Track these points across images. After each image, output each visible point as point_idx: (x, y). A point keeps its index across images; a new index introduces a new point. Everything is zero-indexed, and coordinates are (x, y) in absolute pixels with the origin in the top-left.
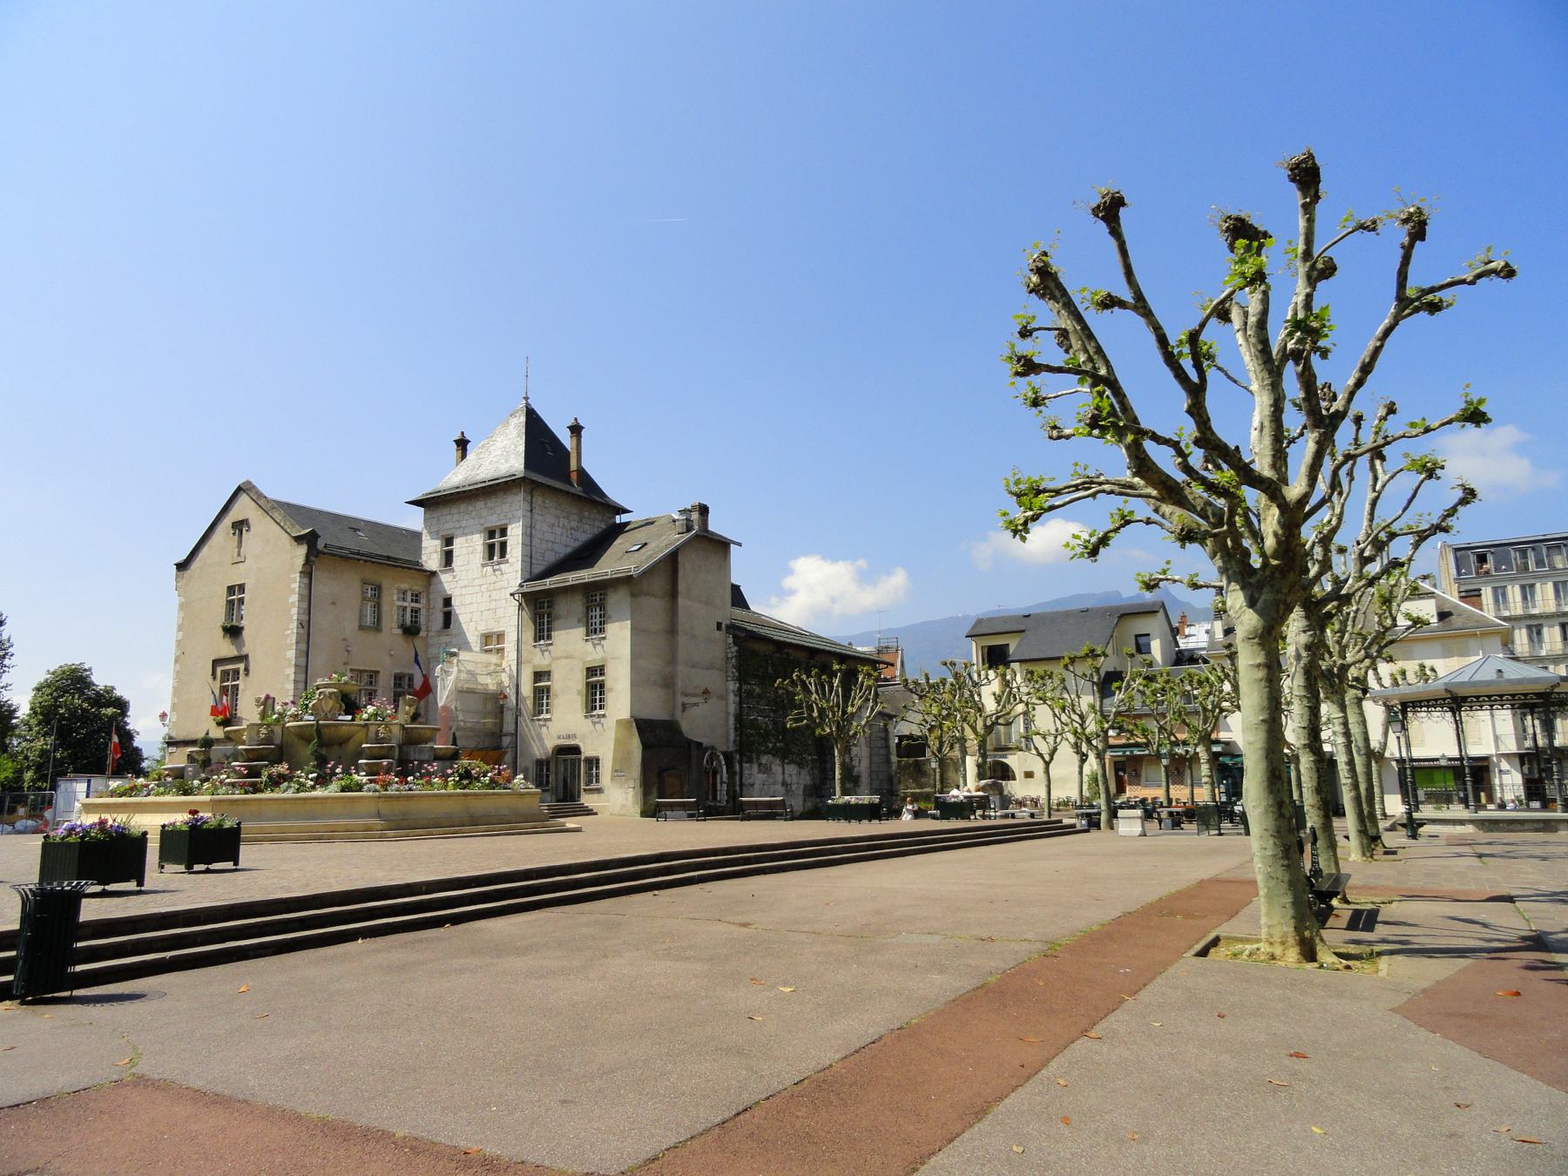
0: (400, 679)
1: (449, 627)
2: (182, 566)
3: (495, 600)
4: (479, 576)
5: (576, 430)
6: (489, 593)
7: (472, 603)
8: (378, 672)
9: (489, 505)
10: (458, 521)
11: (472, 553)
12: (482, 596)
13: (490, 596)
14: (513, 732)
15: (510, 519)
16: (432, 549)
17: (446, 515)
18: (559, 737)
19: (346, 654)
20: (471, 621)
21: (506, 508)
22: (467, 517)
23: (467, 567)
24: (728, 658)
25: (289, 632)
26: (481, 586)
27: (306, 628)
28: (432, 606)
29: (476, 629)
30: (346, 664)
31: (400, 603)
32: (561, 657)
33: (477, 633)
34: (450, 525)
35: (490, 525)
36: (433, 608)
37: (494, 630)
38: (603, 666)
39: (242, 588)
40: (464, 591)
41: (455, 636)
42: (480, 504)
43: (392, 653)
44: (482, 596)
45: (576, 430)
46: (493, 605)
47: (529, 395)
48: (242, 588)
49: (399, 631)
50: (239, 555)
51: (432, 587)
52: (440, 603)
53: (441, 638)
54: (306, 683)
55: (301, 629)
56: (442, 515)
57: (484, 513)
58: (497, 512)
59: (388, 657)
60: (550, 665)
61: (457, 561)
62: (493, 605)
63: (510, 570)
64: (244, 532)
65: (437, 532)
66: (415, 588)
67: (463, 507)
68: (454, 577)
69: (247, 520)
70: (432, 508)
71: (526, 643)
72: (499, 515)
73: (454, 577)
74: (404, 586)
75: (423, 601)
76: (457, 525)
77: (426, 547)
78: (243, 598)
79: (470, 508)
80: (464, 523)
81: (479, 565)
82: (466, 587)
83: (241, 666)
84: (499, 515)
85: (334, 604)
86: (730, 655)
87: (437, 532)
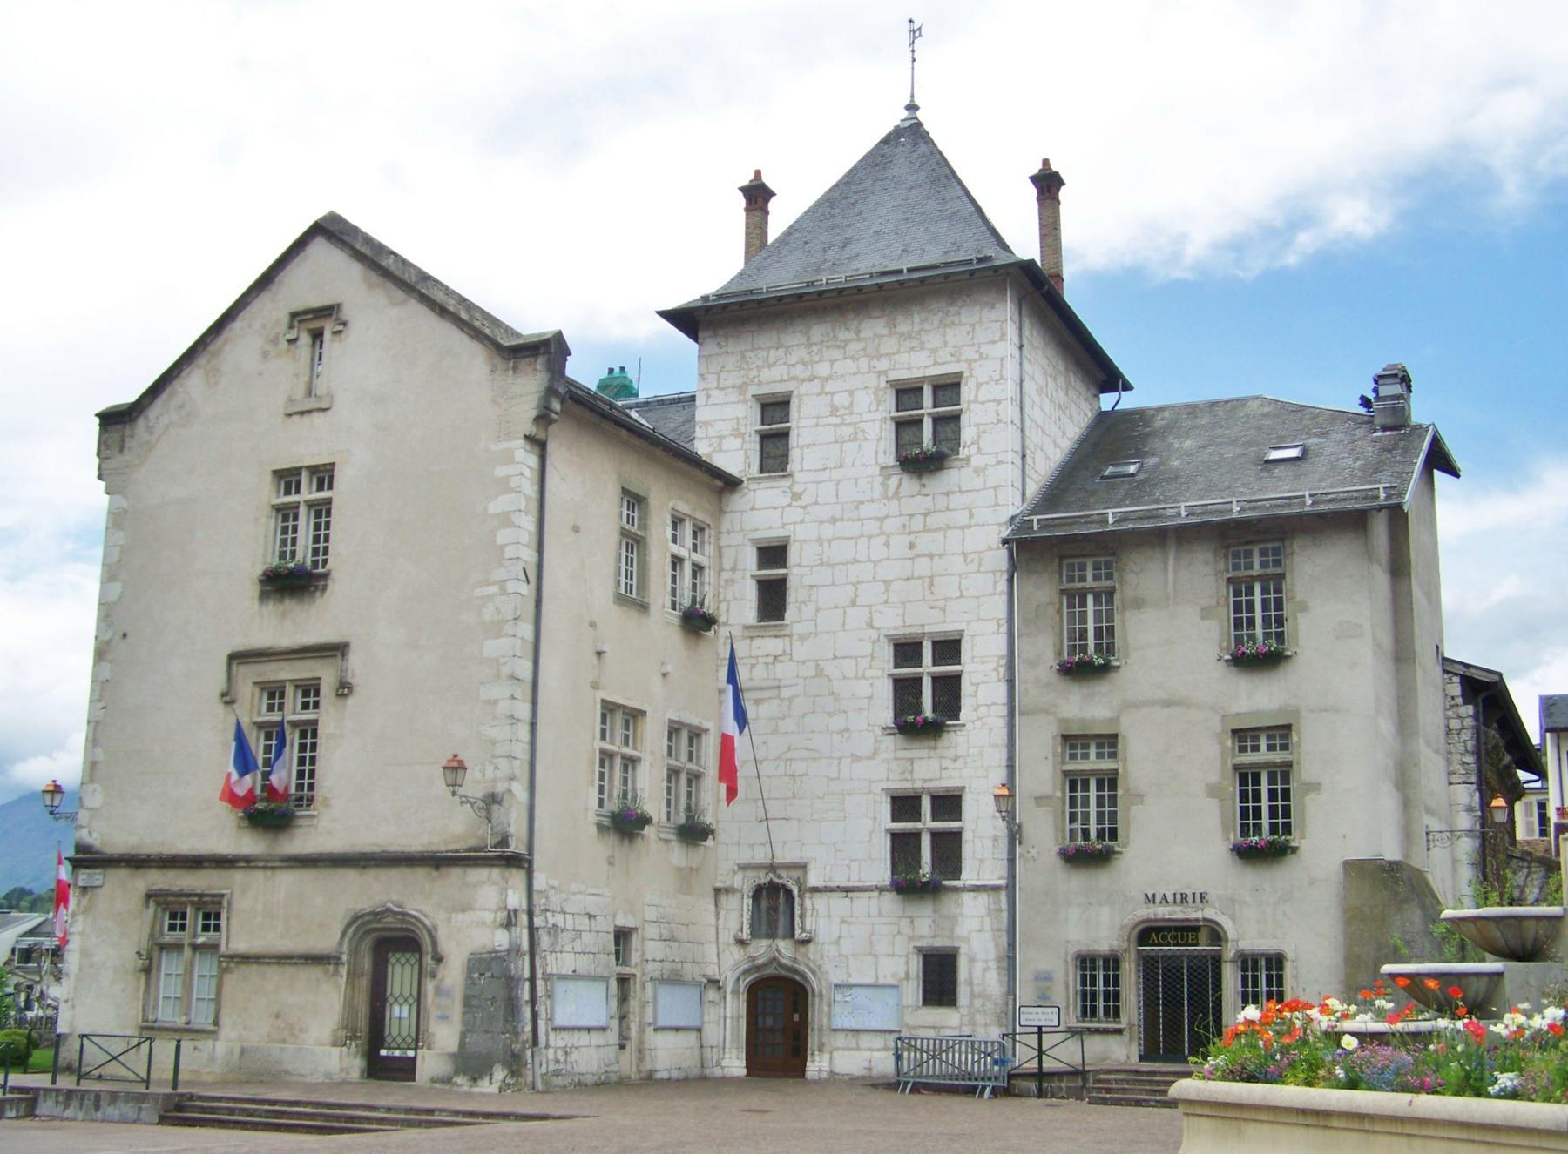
0: (677, 731)
1: (781, 617)
2: (115, 421)
3: (931, 556)
4: (877, 494)
5: (1048, 184)
6: (911, 538)
7: (856, 561)
8: (643, 713)
9: (903, 327)
10: (804, 364)
11: (854, 438)
12: (887, 544)
13: (912, 546)
14: (1003, 882)
15: (970, 362)
16: (725, 428)
17: (769, 349)
18: (1150, 900)
19: (595, 660)
20: (854, 603)
21: (956, 336)
22: (836, 354)
23: (836, 474)
24: (1449, 731)
25: (494, 589)
26: (881, 520)
27: (533, 578)
28: (727, 564)
29: (871, 625)
30: (595, 686)
31: (675, 549)
32: (1151, 703)
33: (873, 634)
34: (779, 372)
35: (905, 375)
36: (734, 569)
37: (927, 629)
38: (1288, 727)
39: (324, 475)
40: (827, 531)
41: (802, 638)
42: (874, 327)
43: (669, 668)
44: (887, 544)
45: (1048, 184)
46: (923, 567)
47: (917, 102)
48: (324, 475)
49: (675, 617)
50: (309, 392)
51: (728, 517)
52: (750, 558)
53: (757, 642)
54: (533, 725)
55: (525, 584)
56: (753, 349)
57: (889, 345)
58: (930, 346)
59: (657, 678)
60: (1115, 720)
61: (800, 457)
62: (923, 567)
63: (977, 482)
64: (327, 335)
65: (742, 388)
66: (699, 515)
67: (818, 331)
68: (796, 496)
69: (339, 305)
70: (721, 332)
71: (1033, 664)
72: (934, 351)
73: (796, 496)
74: (683, 508)
75: (709, 549)
76: (799, 371)
77: (706, 424)
78: (329, 501)
79: (843, 335)
80: (823, 369)
81: (877, 470)
82: (834, 520)
83: (327, 674)
84: (934, 351)
85: (576, 529)
86: (1455, 724)
87: (742, 388)
